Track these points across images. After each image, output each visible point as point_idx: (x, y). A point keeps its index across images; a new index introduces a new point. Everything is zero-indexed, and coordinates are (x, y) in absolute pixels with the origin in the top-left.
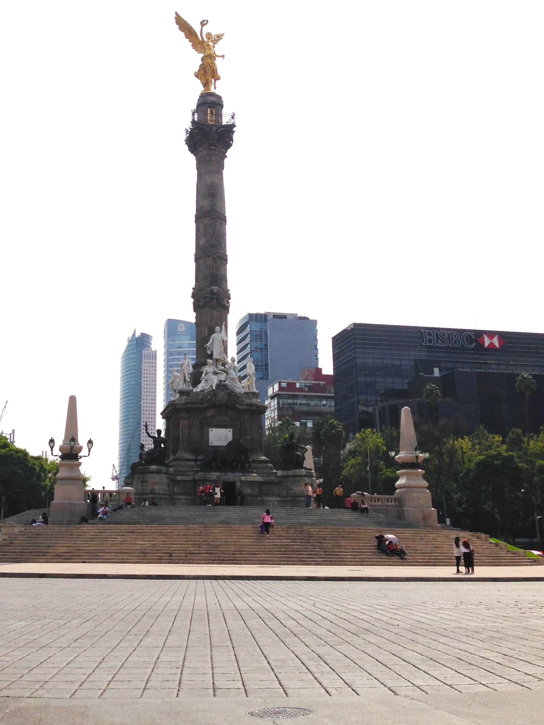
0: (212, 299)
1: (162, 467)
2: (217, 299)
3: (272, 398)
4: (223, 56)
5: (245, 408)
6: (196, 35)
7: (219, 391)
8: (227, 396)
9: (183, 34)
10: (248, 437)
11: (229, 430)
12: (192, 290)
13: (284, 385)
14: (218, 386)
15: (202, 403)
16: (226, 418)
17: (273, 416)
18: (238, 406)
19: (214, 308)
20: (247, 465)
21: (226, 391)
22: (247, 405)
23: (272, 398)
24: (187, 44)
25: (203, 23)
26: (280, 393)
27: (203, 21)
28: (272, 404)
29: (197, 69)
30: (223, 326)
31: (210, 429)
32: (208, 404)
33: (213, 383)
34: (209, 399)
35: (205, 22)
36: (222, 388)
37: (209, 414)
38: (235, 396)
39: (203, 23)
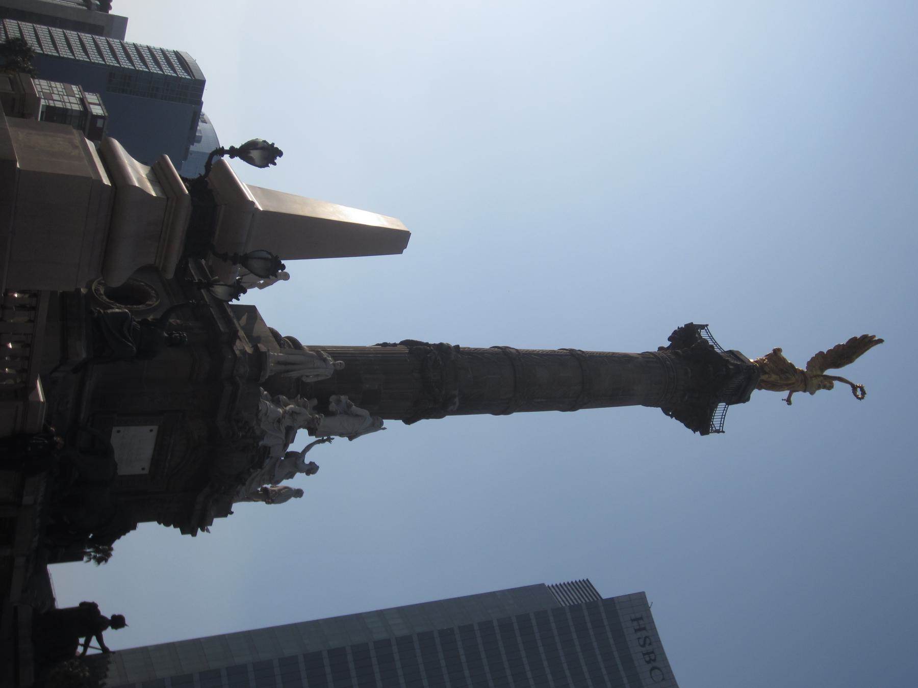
3: (82, 101)
4: (789, 401)
6: (837, 365)
9: (843, 342)
11: (147, 465)
13: (100, 123)
17: (56, 97)
23: (82, 101)
24: (826, 347)
25: (858, 391)
26: (89, 117)
27: (863, 393)
28: (73, 100)
29: (789, 355)
31: (155, 428)
35: (859, 393)
39: (858, 391)
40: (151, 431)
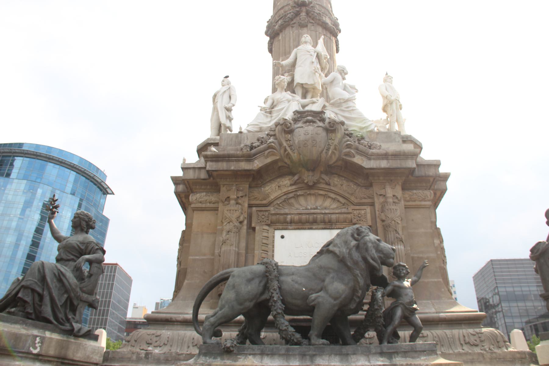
0: (297, 14)
1: (35, 332)
2: (308, 13)
5: (384, 164)
7: (300, 124)
8: (324, 134)
10: (399, 247)
12: (267, 24)
14: (300, 116)
15: (249, 158)
16: (328, 203)
18: (358, 160)
19: (303, 26)
20: (405, 334)
21: (321, 124)
22: (385, 156)
30: (321, 41)
32: (269, 160)
33: (285, 114)
34: (269, 147)
36: (310, 118)
37: (275, 190)
38: (350, 135)
40: (282, 237)
